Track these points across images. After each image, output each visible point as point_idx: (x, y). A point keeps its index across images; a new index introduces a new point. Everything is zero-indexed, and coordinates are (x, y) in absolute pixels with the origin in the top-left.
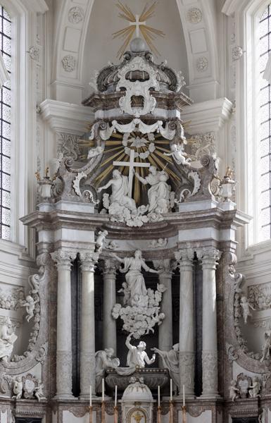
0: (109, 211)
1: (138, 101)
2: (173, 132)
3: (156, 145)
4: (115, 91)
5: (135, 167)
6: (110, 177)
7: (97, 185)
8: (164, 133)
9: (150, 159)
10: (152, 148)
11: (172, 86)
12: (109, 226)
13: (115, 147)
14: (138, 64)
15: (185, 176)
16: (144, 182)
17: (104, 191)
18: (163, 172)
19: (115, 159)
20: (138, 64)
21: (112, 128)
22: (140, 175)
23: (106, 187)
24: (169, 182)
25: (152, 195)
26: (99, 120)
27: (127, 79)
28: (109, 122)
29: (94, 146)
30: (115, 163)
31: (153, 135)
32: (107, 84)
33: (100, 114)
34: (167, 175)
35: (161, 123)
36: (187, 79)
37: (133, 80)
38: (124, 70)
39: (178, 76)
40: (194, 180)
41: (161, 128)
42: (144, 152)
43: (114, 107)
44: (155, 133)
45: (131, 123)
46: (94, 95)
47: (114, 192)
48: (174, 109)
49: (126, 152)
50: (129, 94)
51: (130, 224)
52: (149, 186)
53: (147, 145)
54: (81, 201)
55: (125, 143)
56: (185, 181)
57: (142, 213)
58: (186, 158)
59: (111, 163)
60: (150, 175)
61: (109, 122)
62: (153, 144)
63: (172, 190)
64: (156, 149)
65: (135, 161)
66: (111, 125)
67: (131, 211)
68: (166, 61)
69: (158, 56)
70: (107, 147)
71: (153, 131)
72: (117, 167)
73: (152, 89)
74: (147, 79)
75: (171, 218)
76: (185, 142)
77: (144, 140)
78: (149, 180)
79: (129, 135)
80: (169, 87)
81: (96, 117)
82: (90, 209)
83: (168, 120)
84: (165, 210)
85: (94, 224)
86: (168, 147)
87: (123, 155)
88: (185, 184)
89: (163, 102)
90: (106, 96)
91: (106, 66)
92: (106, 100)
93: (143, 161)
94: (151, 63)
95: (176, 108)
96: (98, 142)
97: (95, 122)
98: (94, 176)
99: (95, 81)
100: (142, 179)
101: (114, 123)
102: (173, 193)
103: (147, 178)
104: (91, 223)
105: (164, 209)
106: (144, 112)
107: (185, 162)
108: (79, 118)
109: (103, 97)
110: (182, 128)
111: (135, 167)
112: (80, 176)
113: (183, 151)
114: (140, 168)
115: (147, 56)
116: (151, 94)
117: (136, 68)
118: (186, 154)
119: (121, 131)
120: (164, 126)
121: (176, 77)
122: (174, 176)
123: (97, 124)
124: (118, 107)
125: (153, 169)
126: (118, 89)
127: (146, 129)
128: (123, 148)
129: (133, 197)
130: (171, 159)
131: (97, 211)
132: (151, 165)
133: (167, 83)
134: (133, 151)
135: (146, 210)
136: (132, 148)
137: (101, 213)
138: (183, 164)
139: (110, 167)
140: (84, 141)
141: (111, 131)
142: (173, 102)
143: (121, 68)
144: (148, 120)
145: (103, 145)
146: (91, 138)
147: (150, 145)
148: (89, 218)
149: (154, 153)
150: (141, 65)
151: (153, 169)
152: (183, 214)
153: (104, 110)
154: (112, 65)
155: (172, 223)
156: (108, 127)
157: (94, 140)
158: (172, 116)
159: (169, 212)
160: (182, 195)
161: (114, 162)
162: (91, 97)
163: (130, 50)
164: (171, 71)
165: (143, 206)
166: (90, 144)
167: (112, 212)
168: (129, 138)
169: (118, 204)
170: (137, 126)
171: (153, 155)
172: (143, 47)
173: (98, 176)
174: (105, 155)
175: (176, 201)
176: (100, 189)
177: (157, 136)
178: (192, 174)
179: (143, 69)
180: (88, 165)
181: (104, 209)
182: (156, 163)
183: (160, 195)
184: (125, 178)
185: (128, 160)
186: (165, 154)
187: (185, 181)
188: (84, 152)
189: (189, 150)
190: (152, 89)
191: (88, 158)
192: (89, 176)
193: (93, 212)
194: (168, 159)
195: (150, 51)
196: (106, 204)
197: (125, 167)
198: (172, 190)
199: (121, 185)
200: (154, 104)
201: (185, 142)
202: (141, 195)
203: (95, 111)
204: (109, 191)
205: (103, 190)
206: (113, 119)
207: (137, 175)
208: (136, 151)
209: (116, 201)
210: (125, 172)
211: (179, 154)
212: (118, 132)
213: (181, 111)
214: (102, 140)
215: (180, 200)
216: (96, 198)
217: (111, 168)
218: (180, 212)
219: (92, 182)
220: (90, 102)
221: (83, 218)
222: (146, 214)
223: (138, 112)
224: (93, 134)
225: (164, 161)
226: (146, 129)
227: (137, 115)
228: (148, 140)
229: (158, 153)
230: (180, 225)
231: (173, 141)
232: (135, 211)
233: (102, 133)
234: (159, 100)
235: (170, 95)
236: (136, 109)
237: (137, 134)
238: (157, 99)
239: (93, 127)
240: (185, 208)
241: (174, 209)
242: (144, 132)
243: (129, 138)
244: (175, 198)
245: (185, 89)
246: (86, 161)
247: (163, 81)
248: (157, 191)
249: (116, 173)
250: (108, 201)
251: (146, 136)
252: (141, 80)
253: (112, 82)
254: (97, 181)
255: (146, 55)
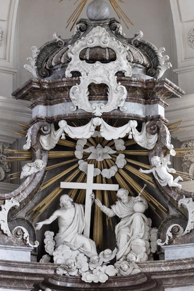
0: (55, 259)
1: (99, 91)
2: (154, 138)
3: (127, 157)
4: (64, 76)
5: (94, 191)
6: (56, 205)
7: (36, 219)
8: (139, 138)
9: (119, 178)
10: (121, 161)
11: (152, 68)
12: (53, 282)
13: (64, 159)
14: (99, 37)
15: (173, 204)
16: (110, 212)
17: (46, 228)
18: (139, 198)
19: (64, 179)
20: (99, 37)
21: (59, 133)
22: (103, 203)
23: (49, 222)
24: (148, 213)
25: (122, 233)
26: (38, 119)
27: (82, 59)
28: (54, 123)
29: (32, 158)
30: (64, 185)
31: (122, 142)
32: (51, 67)
33: (41, 111)
34: (145, 202)
35: (134, 124)
36: (173, 60)
37: (92, 61)
38: (78, 46)
39: (160, 55)
40: (187, 211)
41: (135, 132)
42: (108, 168)
43: (61, 101)
44: (126, 139)
45: (89, 125)
46: (31, 83)
47: (62, 229)
48: (155, 103)
49: (81, 168)
50: (85, 81)
51: (88, 278)
52: (117, 219)
53: (114, 157)
54: (10, 243)
55: (78, 154)
56: (173, 212)
57: (107, 261)
58: (175, 176)
59: (57, 184)
60: (118, 203)
61: (54, 123)
62: (123, 156)
63: (154, 225)
64: (128, 163)
65: (95, 181)
66: (57, 128)
67: (89, 258)
68: (142, 33)
69: (129, 24)
70: (50, 161)
71: (123, 136)
72: (66, 191)
73: (120, 75)
74: (113, 59)
75: (151, 270)
76: (173, 153)
77: (108, 150)
78: (118, 209)
79: (85, 143)
80: (147, 71)
81: (34, 116)
82: (25, 256)
83: (146, 120)
84: (142, 256)
85: (31, 278)
86: (146, 160)
87: (77, 172)
88: (173, 217)
89: (138, 93)
90: (49, 84)
91: (50, 40)
92: (50, 90)
93: (107, 181)
94: (118, 36)
95: (157, 101)
96: (38, 153)
97: (33, 122)
98: (31, 204)
99: (34, 63)
100: (105, 209)
101: (63, 124)
102: (155, 230)
103: (113, 207)
104: (26, 278)
105: (140, 255)
106: (109, 107)
107: (172, 183)
108: (9, 116)
109: (46, 87)
110: (168, 132)
111: (94, 191)
112: (8, 205)
113: (169, 166)
114: (102, 192)
115: (112, 26)
116: (118, 81)
117: (96, 43)
118: (174, 171)
119: (72, 136)
120: (139, 128)
121: (156, 56)
122: (157, 204)
123: (36, 126)
124: (69, 100)
125: (122, 193)
126: (68, 74)
127: (110, 133)
128: (76, 162)
129: (91, 237)
130: (151, 179)
131: (35, 258)
132: (120, 188)
133: (143, 65)
134: (91, 167)
135: (113, 257)
136: (89, 162)
137: (42, 261)
138: (170, 185)
139: (57, 190)
140: (15, 151)
141: (58, 135)
142: (154, 93)
143: (73, 43)
144: (116, 120)
145: (45, 157)
146: (27, 147)
147: (118, 158)
148: (23, 270)
149: (124, 169)
150: (103, 39)
151: (122, 193)
152: (172, 263)
153: (46, 104)
154: (59, 39)
155: (153, 277)
156: (53, 129)
157: (31, 150)
158: (152, 114)
159: (149, 259)
160: (169, 233)
161: (62, 183)
162: (26, 86)
163: (86, 18)
164: (150, 48)
165: (108, 251)
166: (25, 156)
167: (58, 259)
168: (86, 147)
169: (69, 248)
170: (98, 129)
171: (122, 172)
172: (106, 12)
173: (36, 204)
174: (48, 173)
175: (159, 242)
176: (40, 225)
177: (129, 144)
178: (184, 201)
179: (107, 45)
180: (21, 187)
181: (45, 256)
182: (126, 181)
183: (134, 234)
184: (79, 207)
185: (84, 180)
186: (141, 171)
187: (173, 212)
188: (16, 167)
189: (178, 164)
190: (120, 75)
191: (22, 177)
192: (24, 204)
193: (29, 260)
194: (146, 179)
195: (117, 19)
196: (49, 248)
197: (79, 190)
198: (154, 225)
199: (73, 219)
200: (125, 96)
201: (173, 153)
202: (105, 234)
203: (32, 107)
204: (55, 227)
205: (44, 226)
206: (60, 118)
207: (99, 203)
208: (96, 167)
209: (65, 243)
210: (79, 197)
211: (163, 170)
212: (68, 138)
213: (165, 106)
214: (43, 150)
215: (167, 242)
216: (33, 238)
217: (57, 192)
218: (166, 259)
219: (27, 214)
220: (25, 93)
221: (13, 269)
222: (113, 262)
223: (98, 108)
224: (29, 140)
225: (140, 182)
226: (110, 133)
227: (98, 112)
228: (115, 150)
229: (130, 169)
230: (167, 279)
231: (154, 152)
232: (96, 258)
233: (44, 140)
234: (131, 90)
235: (147, 82)
236: (95, 104)
237: (97, 141)
238: (128, 88)
239: (30, 131)
240: (175, 253)
241: (157, 255)
242: (108, 138)
243: (86, 147)
244: (159, 237)
245: (170, 74)
246: (19, 182)
247: (138, 63)
248: (129, 226)
249: (65, 199)
250: (53, 244)
251: (111, 144)
252: (104, 61)
253: (58, 63)
254: (36, 211)
255: (110, 25)
